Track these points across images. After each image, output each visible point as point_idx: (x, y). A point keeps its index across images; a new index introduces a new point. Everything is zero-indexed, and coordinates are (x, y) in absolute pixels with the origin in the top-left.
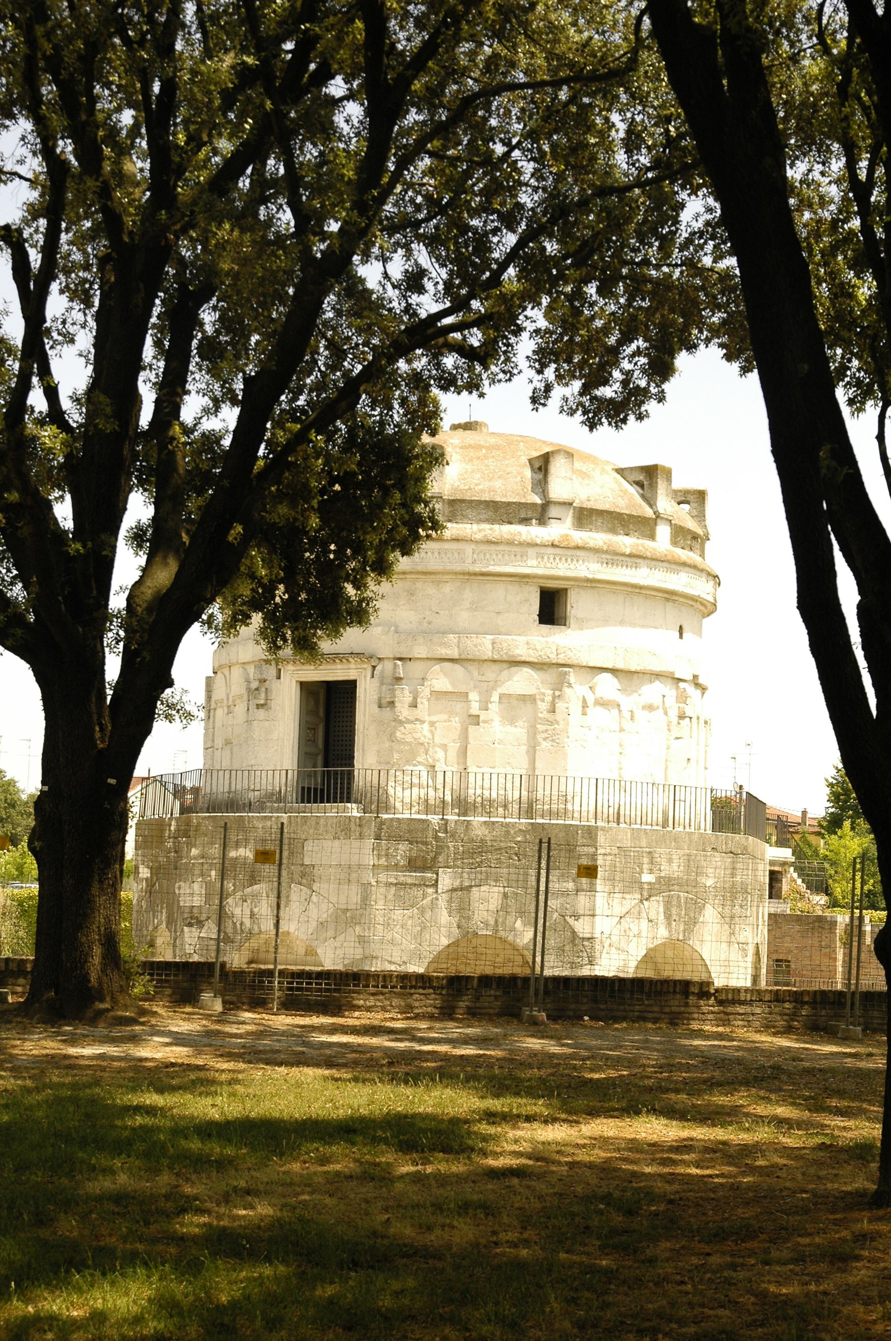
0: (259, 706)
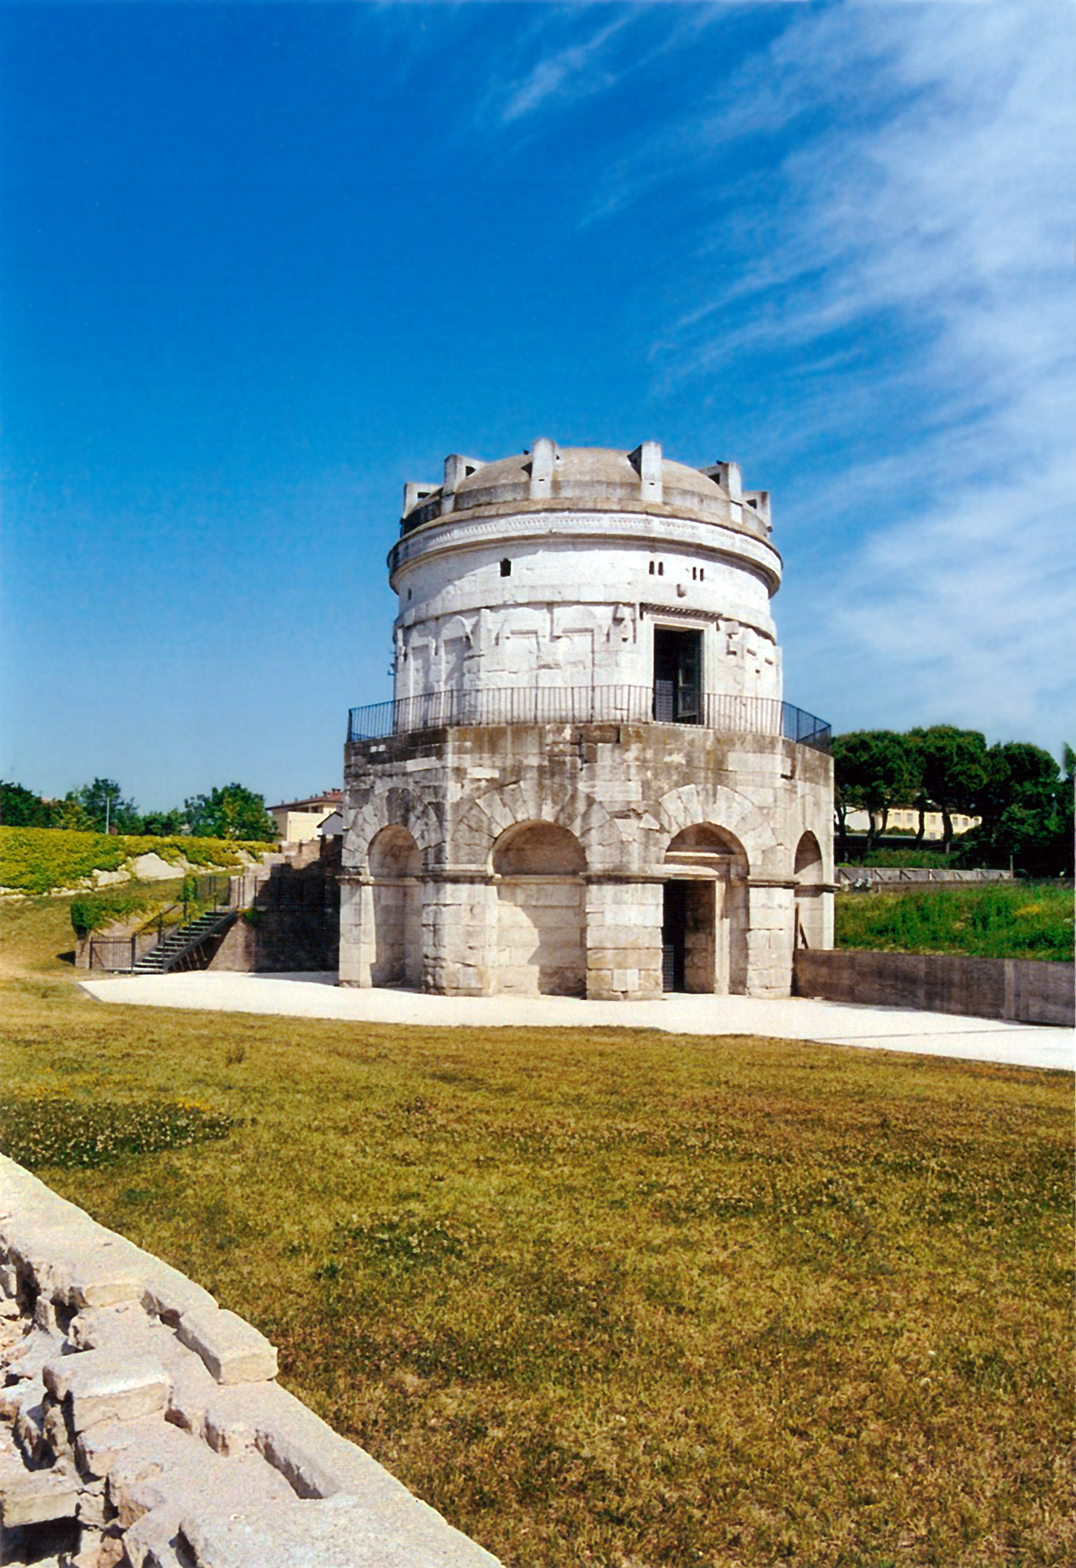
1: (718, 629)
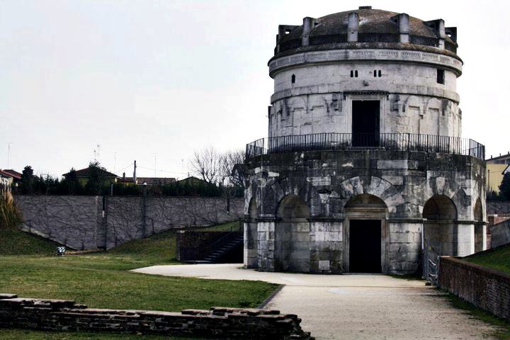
0: (336, 110)
1: (388, 99)
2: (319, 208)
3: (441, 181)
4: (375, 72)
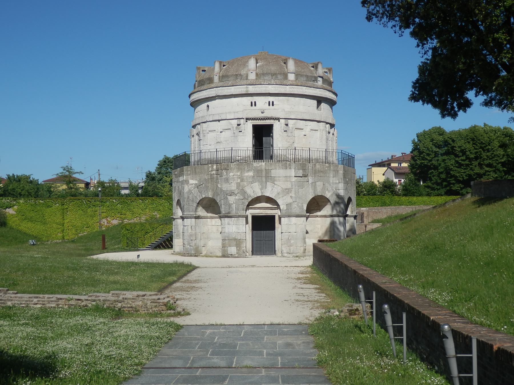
2: (227, 207)
3: (320, 184)
4: (269, 102)
